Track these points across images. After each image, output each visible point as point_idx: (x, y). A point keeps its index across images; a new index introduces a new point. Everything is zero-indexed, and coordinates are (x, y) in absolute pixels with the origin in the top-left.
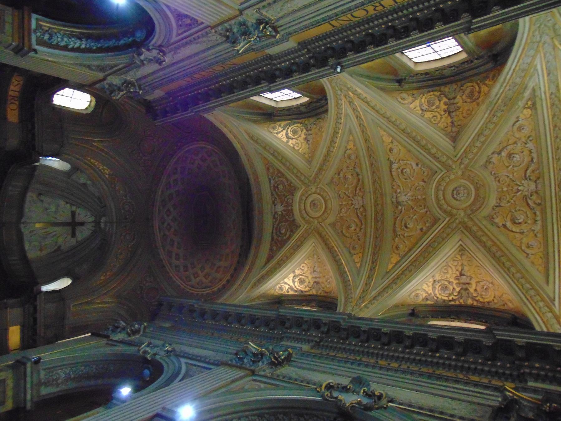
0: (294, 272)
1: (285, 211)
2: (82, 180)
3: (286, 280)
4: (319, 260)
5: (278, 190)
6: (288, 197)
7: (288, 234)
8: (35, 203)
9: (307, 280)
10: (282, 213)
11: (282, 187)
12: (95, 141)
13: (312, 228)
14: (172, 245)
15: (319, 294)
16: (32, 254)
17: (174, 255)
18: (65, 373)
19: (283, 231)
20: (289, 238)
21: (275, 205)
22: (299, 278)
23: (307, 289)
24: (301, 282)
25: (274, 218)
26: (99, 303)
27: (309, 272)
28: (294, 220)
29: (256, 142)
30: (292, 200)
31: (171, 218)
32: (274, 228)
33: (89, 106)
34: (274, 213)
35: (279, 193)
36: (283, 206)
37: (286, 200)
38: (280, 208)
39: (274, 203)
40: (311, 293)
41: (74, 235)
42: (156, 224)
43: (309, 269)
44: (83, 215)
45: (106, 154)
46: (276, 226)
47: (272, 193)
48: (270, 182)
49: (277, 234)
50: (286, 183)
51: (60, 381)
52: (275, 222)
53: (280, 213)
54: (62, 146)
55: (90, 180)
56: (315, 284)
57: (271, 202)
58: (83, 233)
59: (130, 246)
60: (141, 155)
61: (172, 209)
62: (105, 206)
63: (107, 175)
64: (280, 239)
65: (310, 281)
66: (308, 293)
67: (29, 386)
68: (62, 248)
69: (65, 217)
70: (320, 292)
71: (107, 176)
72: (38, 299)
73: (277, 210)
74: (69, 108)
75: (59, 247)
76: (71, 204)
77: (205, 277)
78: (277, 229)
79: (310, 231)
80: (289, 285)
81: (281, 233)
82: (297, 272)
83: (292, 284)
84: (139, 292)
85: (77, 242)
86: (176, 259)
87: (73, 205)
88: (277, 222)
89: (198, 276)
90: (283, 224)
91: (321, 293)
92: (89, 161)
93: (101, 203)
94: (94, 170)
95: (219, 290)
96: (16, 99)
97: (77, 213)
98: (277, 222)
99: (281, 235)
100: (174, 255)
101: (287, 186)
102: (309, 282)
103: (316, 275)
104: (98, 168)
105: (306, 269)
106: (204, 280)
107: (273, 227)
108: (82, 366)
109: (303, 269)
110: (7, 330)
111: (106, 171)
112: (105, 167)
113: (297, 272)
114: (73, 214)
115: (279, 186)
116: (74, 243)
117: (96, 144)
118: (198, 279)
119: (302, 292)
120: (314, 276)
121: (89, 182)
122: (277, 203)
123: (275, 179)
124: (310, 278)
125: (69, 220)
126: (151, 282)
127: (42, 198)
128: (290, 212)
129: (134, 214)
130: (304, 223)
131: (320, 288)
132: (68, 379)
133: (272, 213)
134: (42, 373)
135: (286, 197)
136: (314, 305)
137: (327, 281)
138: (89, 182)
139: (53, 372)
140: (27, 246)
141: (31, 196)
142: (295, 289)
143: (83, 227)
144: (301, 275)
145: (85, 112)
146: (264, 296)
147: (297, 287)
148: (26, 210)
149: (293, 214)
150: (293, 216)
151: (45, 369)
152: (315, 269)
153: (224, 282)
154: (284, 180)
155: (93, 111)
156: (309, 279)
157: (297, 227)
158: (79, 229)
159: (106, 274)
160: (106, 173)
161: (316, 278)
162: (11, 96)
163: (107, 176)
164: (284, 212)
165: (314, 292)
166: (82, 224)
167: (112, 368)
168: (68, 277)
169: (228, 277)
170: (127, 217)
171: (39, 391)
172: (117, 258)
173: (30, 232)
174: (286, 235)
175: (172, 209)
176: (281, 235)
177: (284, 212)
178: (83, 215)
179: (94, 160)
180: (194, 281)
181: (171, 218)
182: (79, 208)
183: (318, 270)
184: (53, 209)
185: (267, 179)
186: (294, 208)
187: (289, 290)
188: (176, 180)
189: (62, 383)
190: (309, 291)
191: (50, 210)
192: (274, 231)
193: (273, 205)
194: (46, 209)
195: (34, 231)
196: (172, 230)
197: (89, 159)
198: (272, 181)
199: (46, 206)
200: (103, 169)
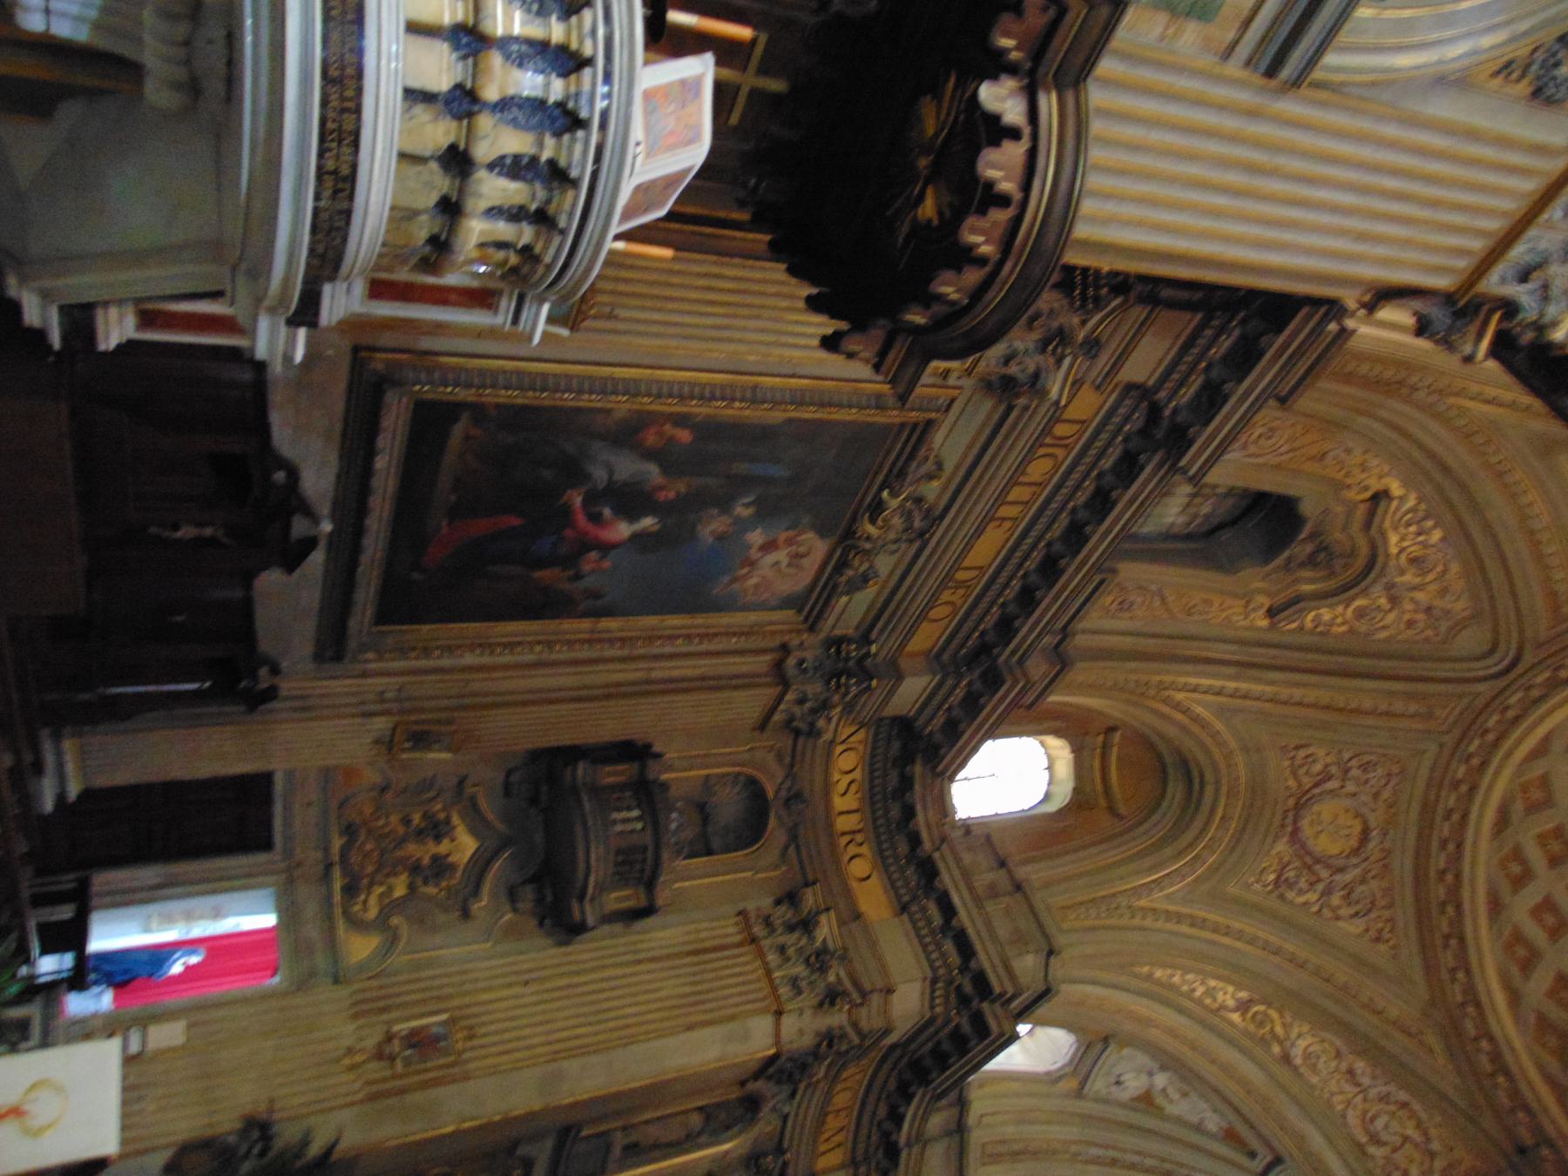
2: (1134, 1084)
12: (1137, 891)
33: (1050, 783)
45: (1192, 925)
54: (1051, 953)
55: (1163, 1068)
60: (1324, 874)
74: (997, 815)
96: (859, 838)
111: (1220, 996)
112: (1212, 983)
117: (1143, 903)
138: (1161, 1080)
145: (1051, 807)
155: (1077, 791)
160: (1223, 1007)
162: (843, 834)
163: (1235, 1017)
179: (1164, 966)
197: (1146, 969)
200: (1210, 992)
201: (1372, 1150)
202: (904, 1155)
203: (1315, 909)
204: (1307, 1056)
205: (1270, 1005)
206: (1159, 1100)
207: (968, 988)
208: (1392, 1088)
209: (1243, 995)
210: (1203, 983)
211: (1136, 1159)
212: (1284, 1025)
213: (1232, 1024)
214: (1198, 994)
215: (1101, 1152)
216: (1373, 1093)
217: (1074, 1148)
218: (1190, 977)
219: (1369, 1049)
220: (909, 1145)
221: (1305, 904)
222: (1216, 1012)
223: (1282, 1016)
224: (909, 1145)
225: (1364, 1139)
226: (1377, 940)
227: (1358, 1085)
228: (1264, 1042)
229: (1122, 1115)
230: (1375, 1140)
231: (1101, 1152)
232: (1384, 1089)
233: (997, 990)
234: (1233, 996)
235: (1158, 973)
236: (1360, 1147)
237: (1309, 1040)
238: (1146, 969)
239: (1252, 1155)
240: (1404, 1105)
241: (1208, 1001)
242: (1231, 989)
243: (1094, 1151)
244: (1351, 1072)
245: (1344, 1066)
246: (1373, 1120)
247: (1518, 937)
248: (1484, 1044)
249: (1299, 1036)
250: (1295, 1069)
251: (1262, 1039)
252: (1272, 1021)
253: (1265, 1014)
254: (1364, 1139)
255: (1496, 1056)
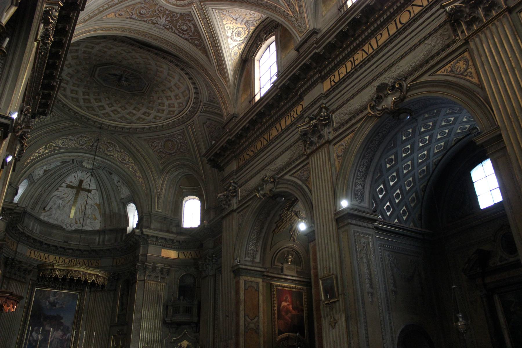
0: (227, 37)
1: (167, 18)
2: (41, 172)
3: (231, 47)
4: (230, 12)
5: (144, 14)
6: (156, 9)
7: (190, 25)
8: (51, 215)
9: (240, 29)
10: (167, 21)
11: (144, 10)
13: (198, 3)
14: (134, 115)
15: (256, 25)
16: (97, 225)
17: (143, 117)
18: (251, 246)
19: (185, 28)
20: (195, 25)
21: (157, 23)
22: (234, 35)
23: (247, 33)
24: (239, 34)
25: (168, 29)
26: (162, 189)
27: (234, 24)
28: (181, 14)
29: (90, 18)
30: (161, 6)
31: (106, 107)
32: (178, 33)
34: (164, 28)
35: (148, 15)
36: (161, 17)
37: (158, 12)
38: (162, 21)
39: (154, 23)
40: (251, 31)
41: (89, 191)
42: (107, 122)
43: (232, 23)
44: (73, 179)
46: (176, 31)
47: (144, 21)
48: (133, 19)
49: (185, 34)
50: (142, 5)
51: (255, 250)
52: (172, 29)
53: (167, 22)
56: (246, 24)
57: (153, 26)
58: (91, 183)
59: (119, 150)
61: (100, 104)
62: (73, 160)
63: (45, 151)
64: (191, 34)
65: (242, 27)
66: (251, 33)
67: (253, 268)
68: (98, 203)
69: (71, 193)
70: (255, 24)
71: (47, 151)
72: (147, 233)
73: (163, 23)
75: (96, 204)
76: (60, 187)
77: (177, 99)
78: (181, 32)
79: (200, 6)
80: (236, 46)
81: (187, 30)
82: (229, 34)
83: (236, 43)
84: (164, 155)
85: (97, 190)
86: (148, 116)
87: (61, 185)
88: (174, 29)
89: (173, 104)
90: (178, 24)
91: (257, 24)
92: (28, 163)
93: (69, 162)
94: (38, 161)
95: (196, 93)
97: (70, 184)
98: (174, 29)
99: (188, 31)
100: (143, 117)
101: (146, 6)
102: (242, 28)
103: (240, 20)
104: (37, 158)
105: (230, 25)
106: (179, 101)
107: (176, 34)
108: (252, 235)
109: (229, 28)
110: (163, 258)
111: (41, 151)
112: (37, 151)
113: (229, 34)
114: (68, 186)
115: (142, 12)
116: (97, 192)
118: (176, 105)
119: (246, 37)
120: (240, 21)
121: (45, 168)
122: (156, 21)
123: (132, 13)
124: (239, 26)
125: (75, 190)
126: (159, 143)
127: (47, 208)
128: (171, 14)
129: (90, 138)
130: (189, 7)
131: (253, 23)
132: (256, 245)
133: (162, 29)
134: (247, 259)
135: (156, 11)
136: (265, 36)
137: (251, 15)
139: (248, 253)
140: (89, 229)
141: (43, 216)
142: (242, 41)
143: (85, 182)
144: (233, 32)
146: (235, 71)
147: (241, 39)
148: (56, 223)
149: (175, 12)
150: (177, 13)
151: (245, 258)
152: (235, 19)
153: (192, 87)
154: (139, 5)
156: (240, 27)
157: (190, 14)
158: (85, 186)
159: (138, 176)
160: (43, 152)
161: (242, 21)
163: (47, 151)
164: (169, 19)
165: (252, 28)
166: (81, 182)
167: (262, 217)
168: (128, 205)
169: (189, 82)
170: (91, 144)
171: (256, 263)
172: (126, 164)
173: (76, 224)
174: (190, 27)
175: (100, 104)
176: (188, 31)
177: (169, 19)
178: (73, 179)
179: (28, 159)
180: (176, 109)
181: (106, 107)
182: (65, 181)
183: (237, 16)
184: (61, 201)
185: (129, 20)
186: (169, 9)
187: (240, 47)
188: (72, 91)
189: (257, 248)
190: (249, 32)
191: (61, 204)
192: (181, 35)
193: (157, 25)
194: (59, 206)
195: (76, 220)
196: (119, 110)
198: (133, 17)
199: (56, 206)
200: (39, 153)
201: (83, 147)
202: (25, 232)
203: (39, 121)
204: (62, 144)
205: (49, 143)
206: (48, 169)
207: (8, 212)
208: (77, 136)
209: (44, 147)
210: (36, 153)
211: (54, 180)
212: (54, 144)
213: (47, 153)
214: (37, 156)
215: (48, 185)
216: (76, 139)
217: (43, 190)
218: (33, 155)
219: (69, 135)
220: (24, 230)
221: (37, 122)
222: (43, 155)
223: (52, 143)
224: (24, 230)
225: (81, 147)
226: (54, 116)
227: (73, 140)
228: (55, 150)
229: (44, 177)
230: (83, 145)
231: (48, 185)
232: (76, 137)
233: (14, 208)
234: (43, 149)
235: (28, 161)
236: (82, 148)
237: (60, 141)
238: (26, 163)
239: (69, 162)
240: (81, 136)
241: (40, 154)
242: (41, 148)
243: (46, 187)
244: (70, 139)
245: (68, 140)
246: (79, 142)
247: (73, 98)
248: (83, 118)
249: (58, 142)
250: (63, 148)
251: (54, 149)
252: (52, 145)
253: (50, 145)
254: (81, 147)
255: (86, 118)
